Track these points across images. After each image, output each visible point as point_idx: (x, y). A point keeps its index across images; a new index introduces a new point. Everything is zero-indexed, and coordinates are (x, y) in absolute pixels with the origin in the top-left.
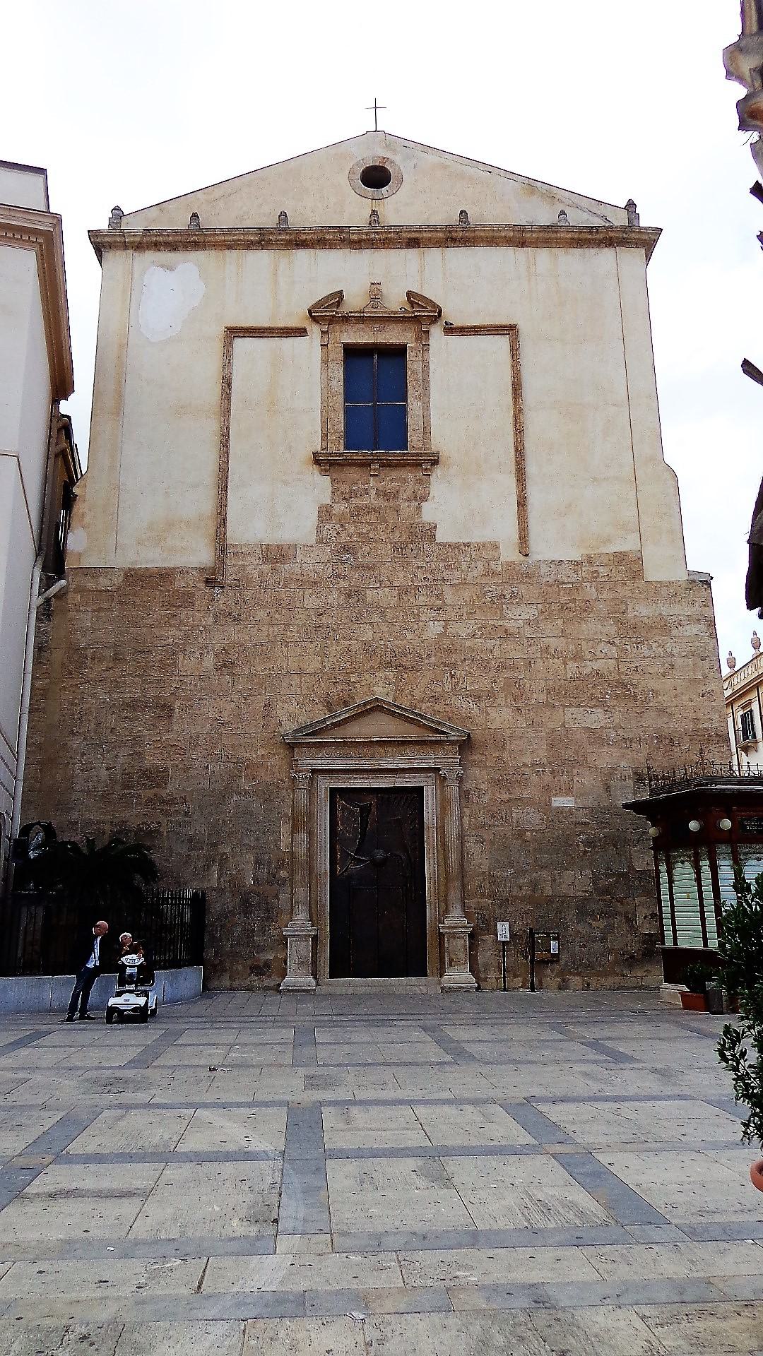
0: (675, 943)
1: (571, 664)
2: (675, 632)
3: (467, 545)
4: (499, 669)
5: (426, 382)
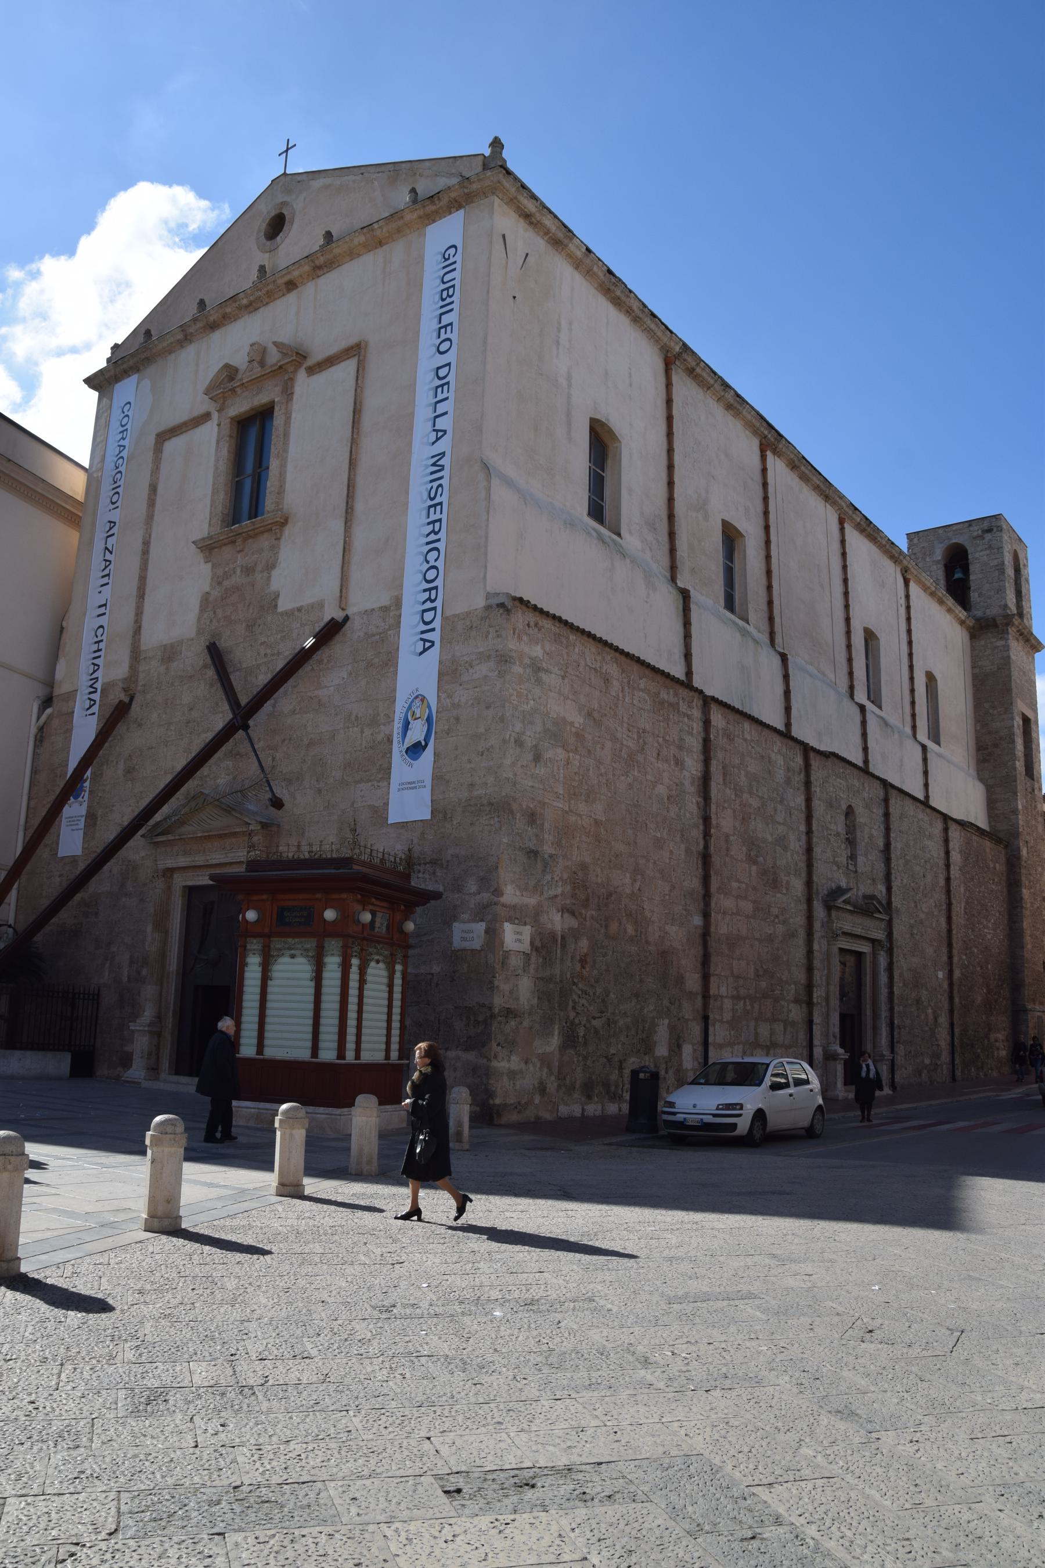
0: (358, 1056)
1: (367, 732)
2: (465, 678)
3: (299, 610)
4: (309, 745)
5: (286, 435)
